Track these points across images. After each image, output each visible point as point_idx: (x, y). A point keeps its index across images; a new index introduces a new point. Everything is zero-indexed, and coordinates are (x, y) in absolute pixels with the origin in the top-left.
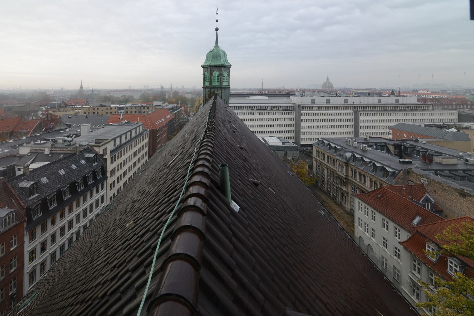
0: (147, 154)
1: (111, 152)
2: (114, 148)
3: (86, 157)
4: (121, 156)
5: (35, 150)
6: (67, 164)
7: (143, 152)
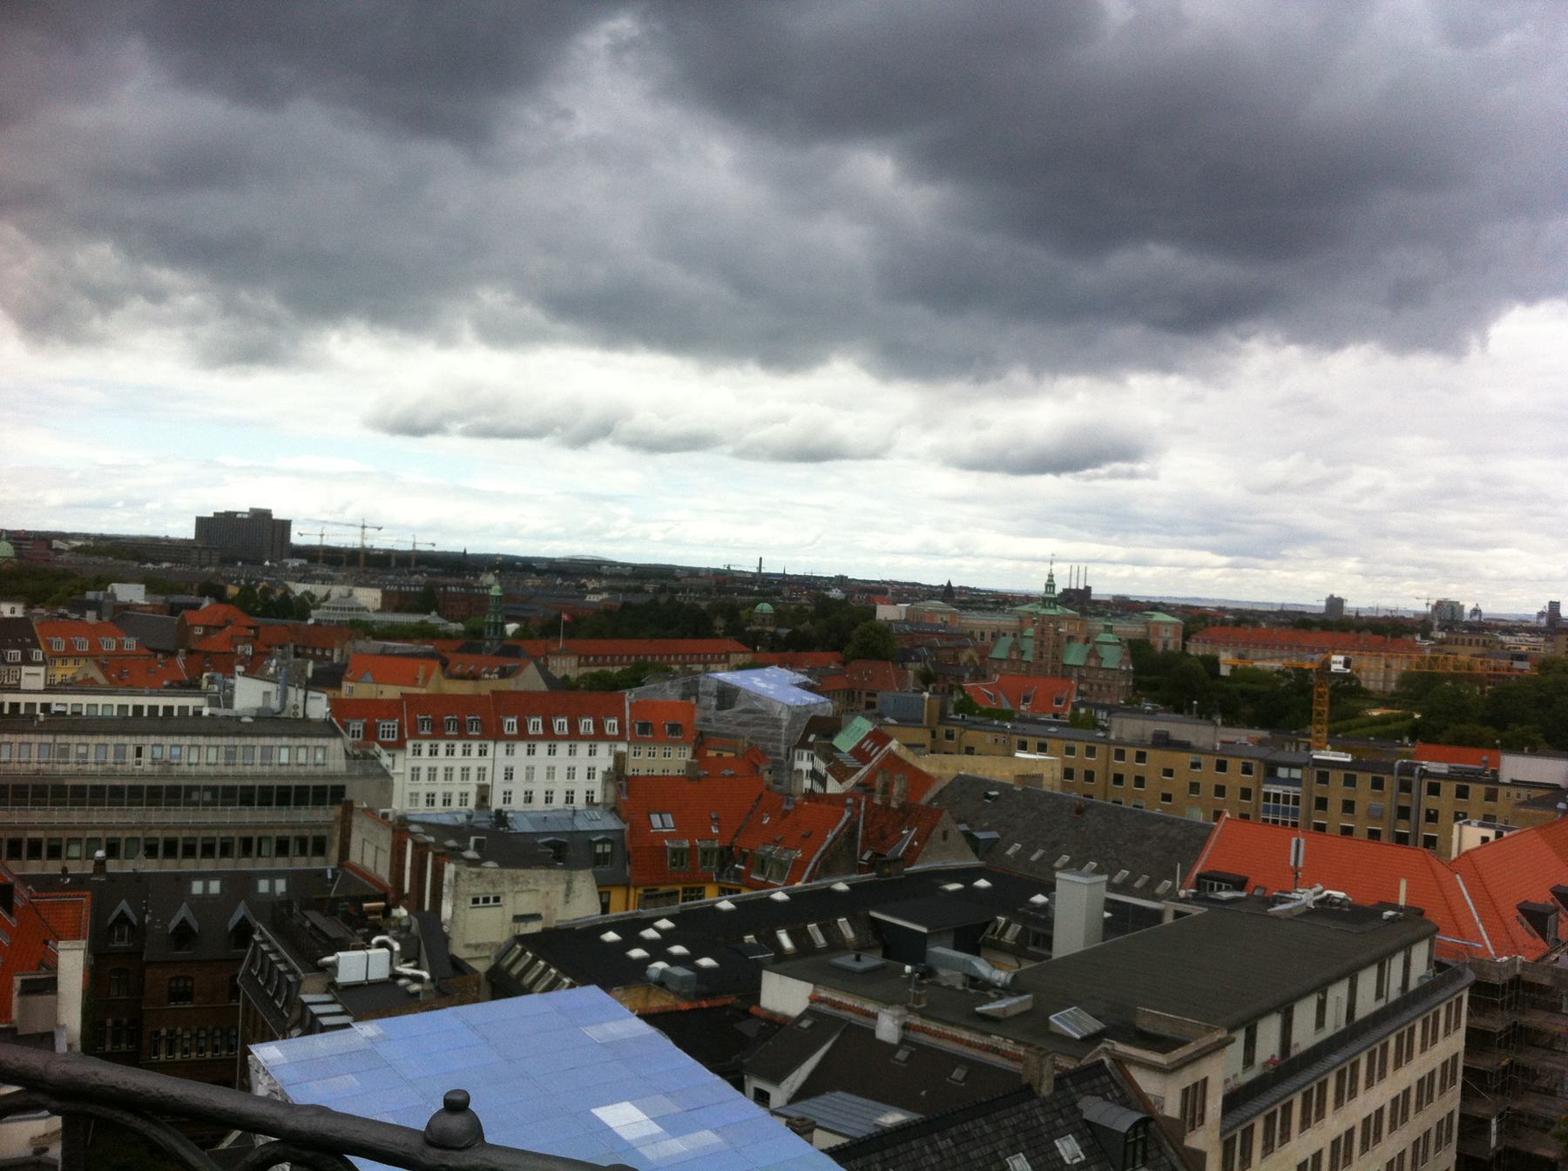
0: (1449, 1136)
1: (1234, 1100)
2: (1251, 1075)
3: (1088, 1124)
4: (1285, 1137)
5: (834, 1004)
6: (989, 1150)
7: (1420, 1122)
